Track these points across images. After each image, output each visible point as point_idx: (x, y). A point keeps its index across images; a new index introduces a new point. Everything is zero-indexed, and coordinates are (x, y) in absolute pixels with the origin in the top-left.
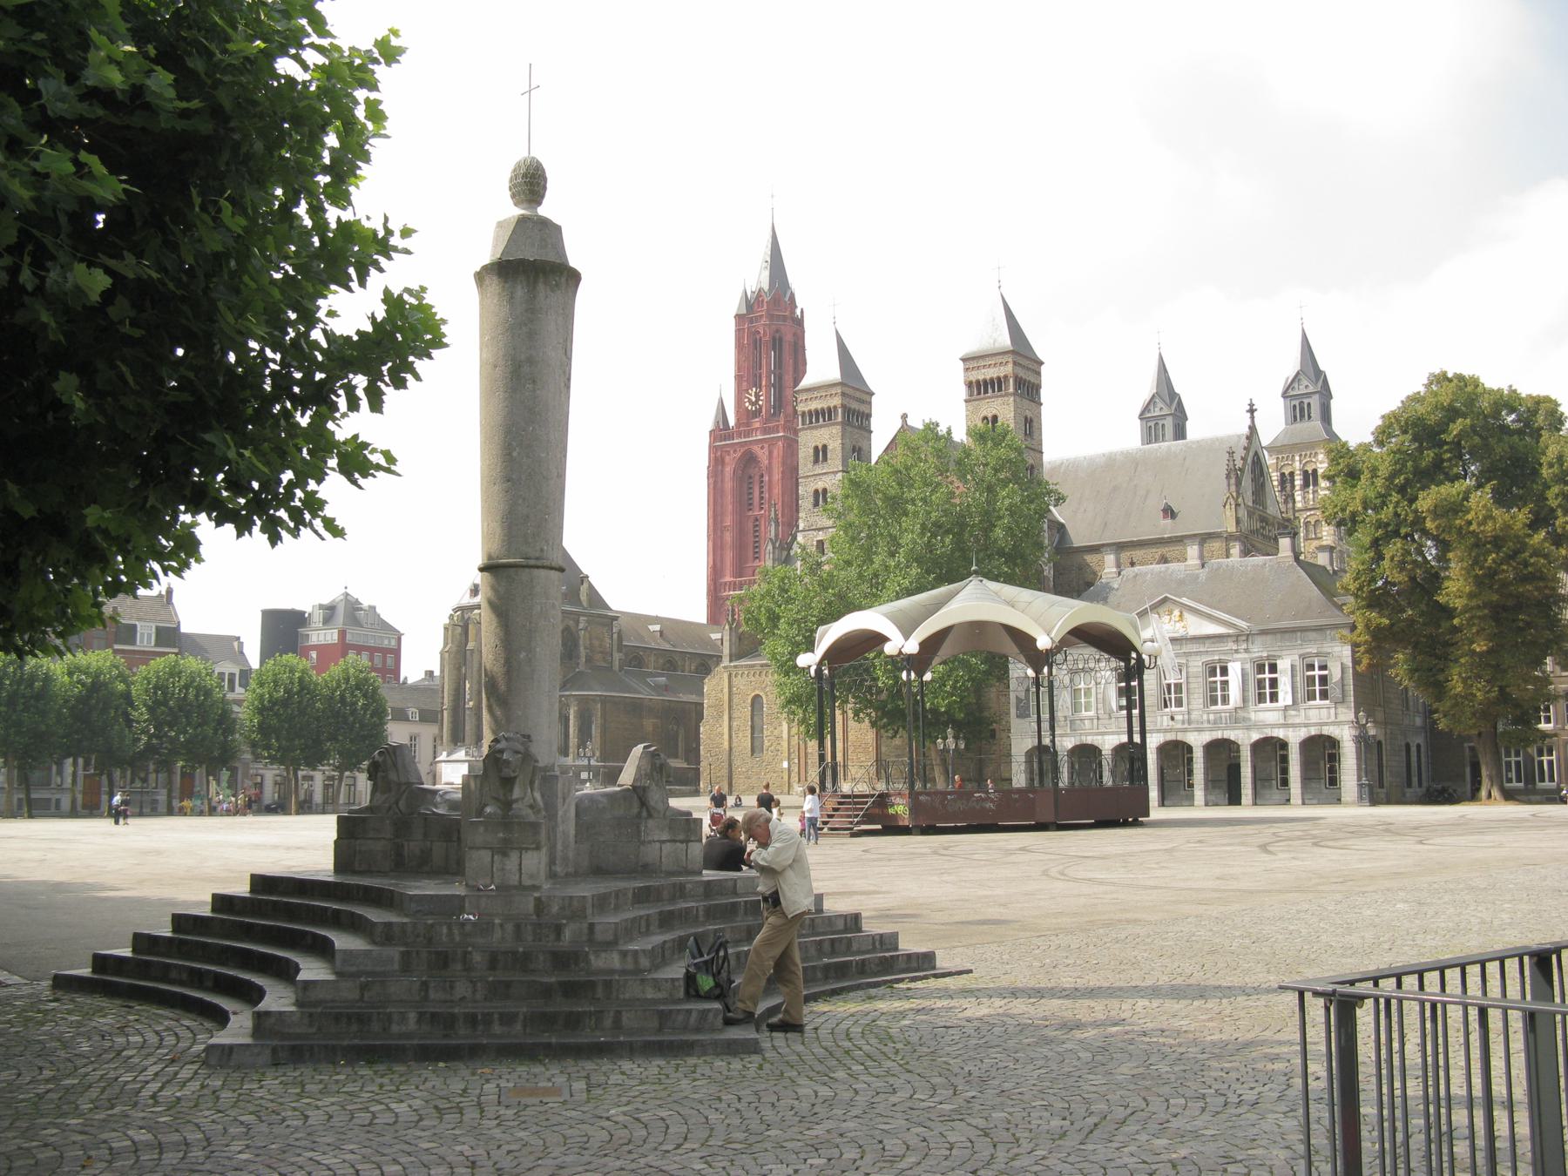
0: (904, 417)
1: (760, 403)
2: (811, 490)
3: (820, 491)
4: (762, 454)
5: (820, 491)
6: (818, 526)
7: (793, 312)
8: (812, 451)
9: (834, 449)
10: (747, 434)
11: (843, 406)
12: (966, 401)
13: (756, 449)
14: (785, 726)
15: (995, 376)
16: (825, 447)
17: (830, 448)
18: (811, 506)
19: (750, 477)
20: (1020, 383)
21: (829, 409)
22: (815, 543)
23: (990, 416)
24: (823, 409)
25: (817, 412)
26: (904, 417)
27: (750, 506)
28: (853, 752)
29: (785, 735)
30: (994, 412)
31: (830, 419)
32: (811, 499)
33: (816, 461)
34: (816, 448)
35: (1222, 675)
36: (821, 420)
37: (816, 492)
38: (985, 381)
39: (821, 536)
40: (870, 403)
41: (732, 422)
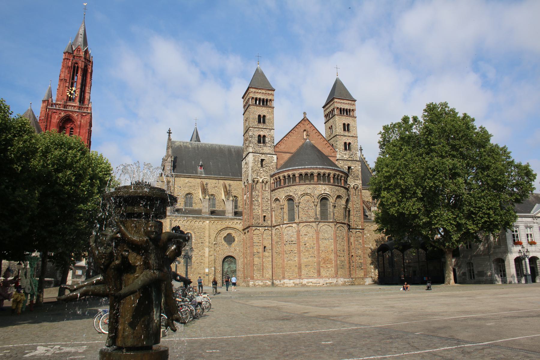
0: (305, 113)
1: (76, 95)
3: (262, 136)
5: (262, 136)
6: (260, 152)
8: (257, 117)
9: (269, 119)
14: (207, 250)
15: (348, 108)
16: (264, 116)
18: (256, 142)
21: (267, 100)
22: (260, 160)
24: (263, 99)
25: (260, 99)
26: (305, 113)
28: (324, 263)
29: (207, 255)
30: (348, 122)
32: (257, 139)
33: (259, 122)
34: (259, 116)
37: (259, 136)
38: (344, 109)
39: (263, 157)
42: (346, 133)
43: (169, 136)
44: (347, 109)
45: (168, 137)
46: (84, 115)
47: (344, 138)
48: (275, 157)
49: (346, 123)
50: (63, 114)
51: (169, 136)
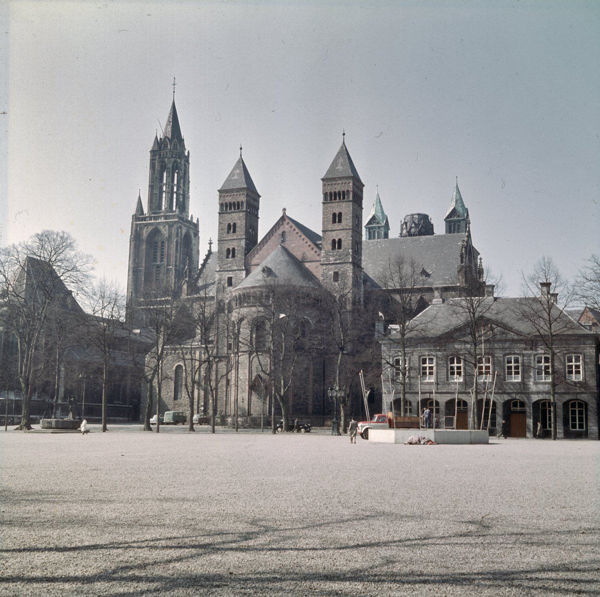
0: (284, 210)
2: (226, 249)
4: (165, 231)
7: (184, 152)
10: (155, 218)
11: (247, 202)
12: (323, 203)
13: (161, 227)
16: (235, 225)
17: (238, 225)
19: (156, 243)
20: (248, 204)
22: (227, 279)
23: (337, 213)
26: (284, 210)
27: (155, 259)
31: (238, 208)
35: (457, 363)
36: (233, 209)
37: (228, 250)
38: (335, 193)
39: (230, 274)
40: (259, 201)
41: (146, 210)
42: (337, 226)
43: (210, 247)
44: (339, 192)
45: (209, 249)
46: (171, 224)
47: (334, 233)
48: (244, 272)
49: (337, 213)
50: (150, 228)
51: (210, 247)
